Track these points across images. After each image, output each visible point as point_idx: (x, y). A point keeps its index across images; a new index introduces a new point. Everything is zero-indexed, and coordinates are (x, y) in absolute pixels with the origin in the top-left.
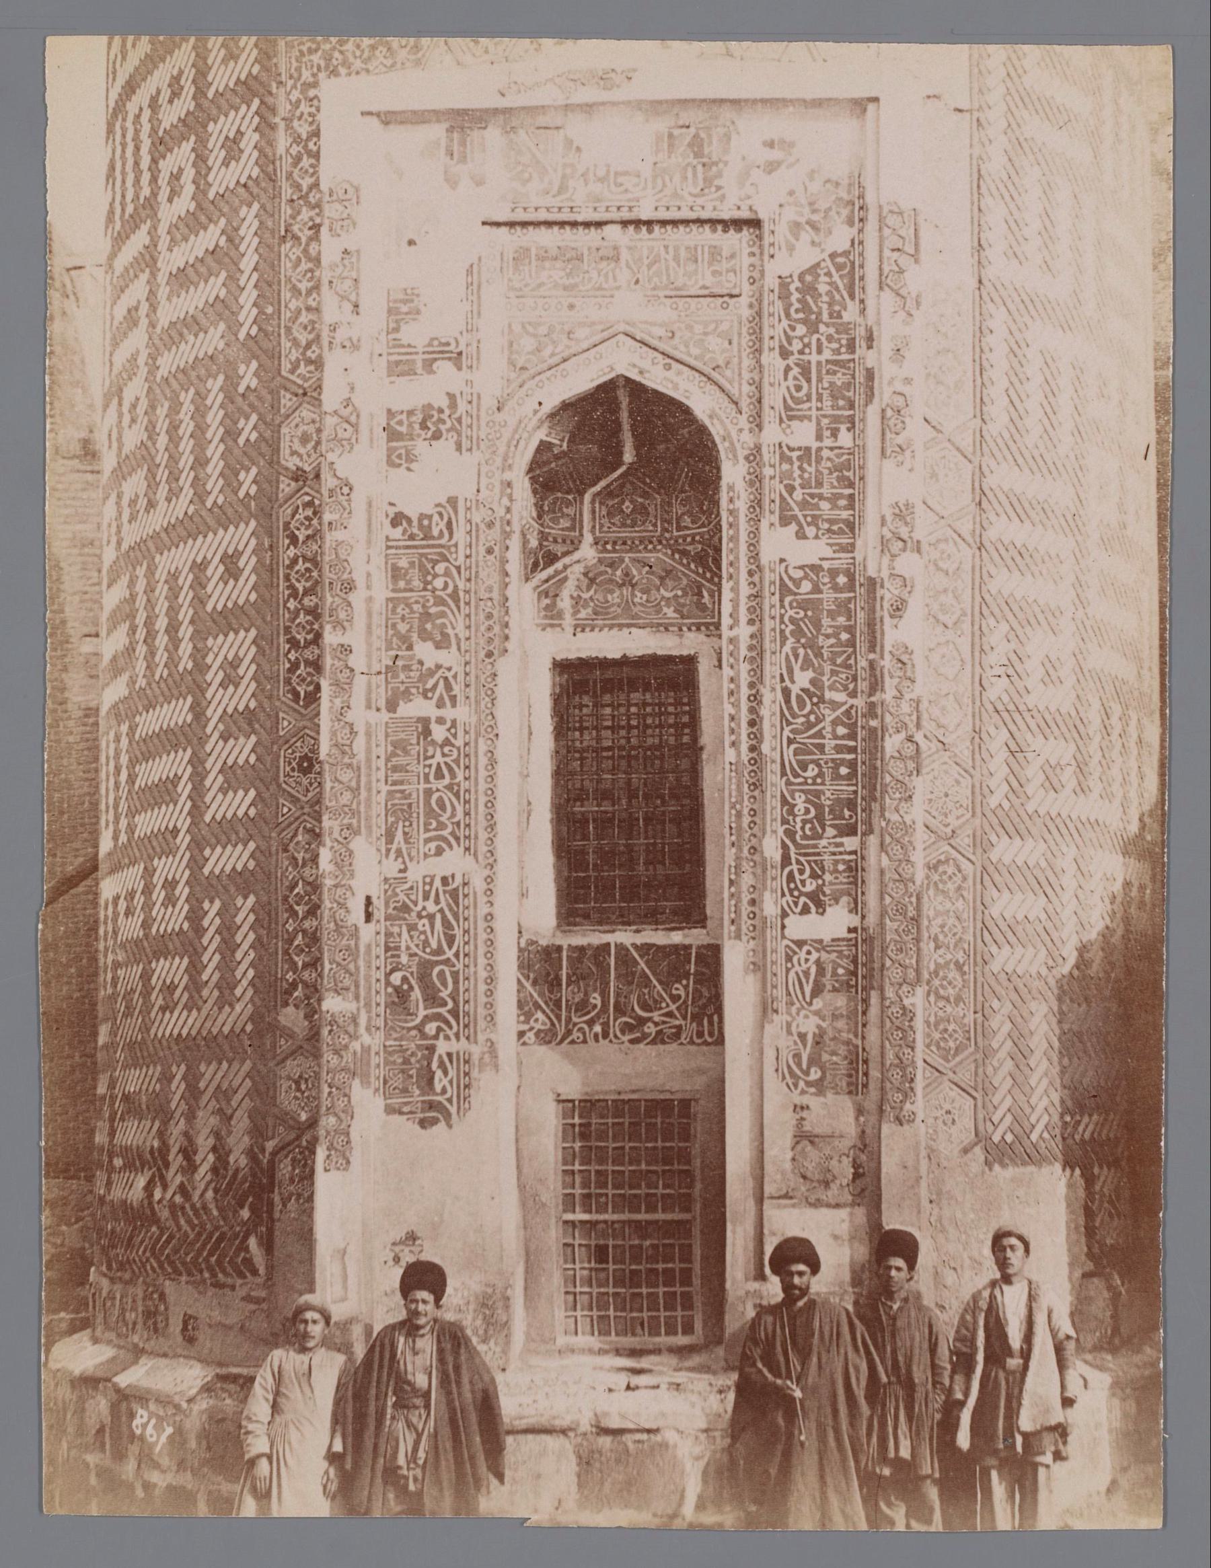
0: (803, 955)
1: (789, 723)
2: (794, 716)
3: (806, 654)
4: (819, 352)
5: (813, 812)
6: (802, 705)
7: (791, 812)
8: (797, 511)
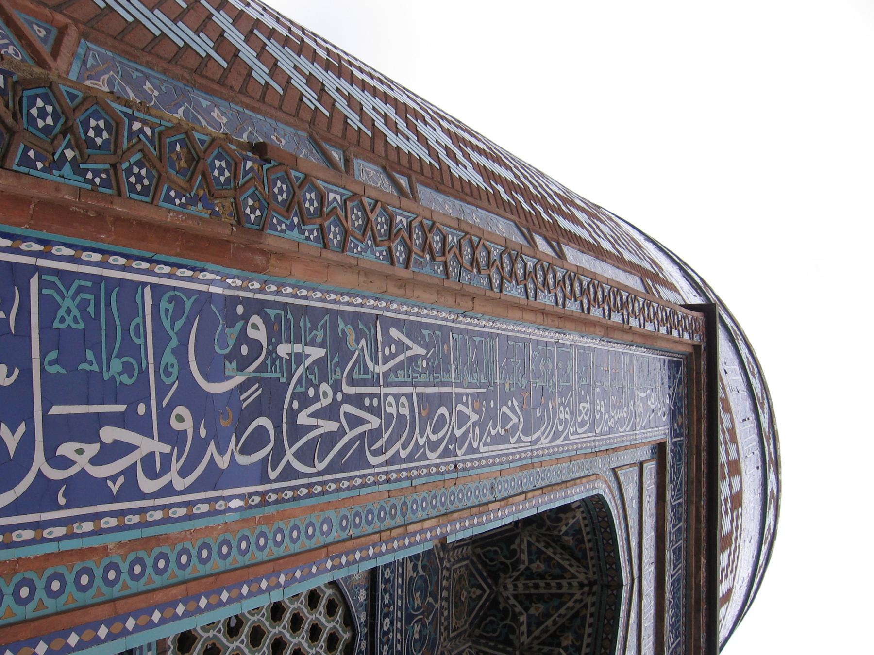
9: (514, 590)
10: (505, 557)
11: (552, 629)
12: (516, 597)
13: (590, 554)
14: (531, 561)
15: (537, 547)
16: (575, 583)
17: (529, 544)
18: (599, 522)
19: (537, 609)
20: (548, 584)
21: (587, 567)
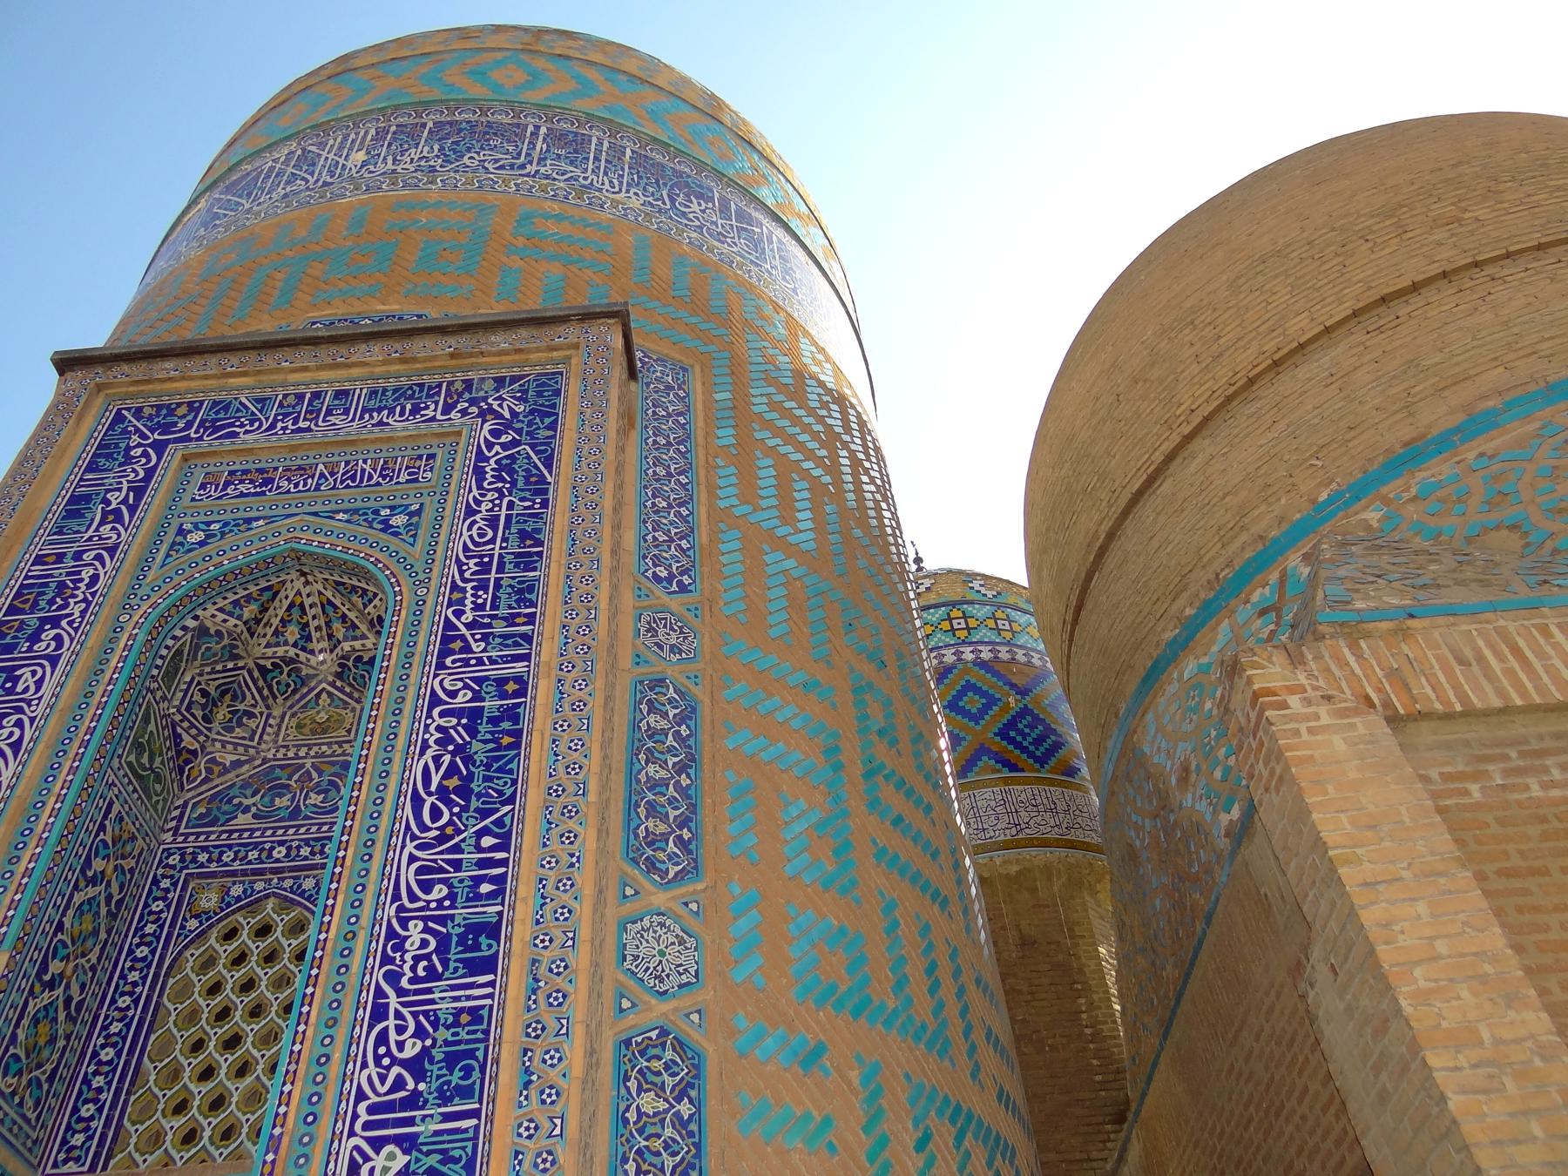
0: (379, 1161)
1: (414, 838)
2: (425, 829)
3: (453, 764)
4: (511, 505)
5: (433, 944)
6: (436, 814)
7: (399, 948)
8: (464, 630)
10: (281, 673)
11: (358, 614)
12: (332, 651)
13: (264, 584)
14: (286, 643)
16: (305, 591)
17: (268, 646)
19: (339, 630)
20: (314, 617)
21: (283, 582)
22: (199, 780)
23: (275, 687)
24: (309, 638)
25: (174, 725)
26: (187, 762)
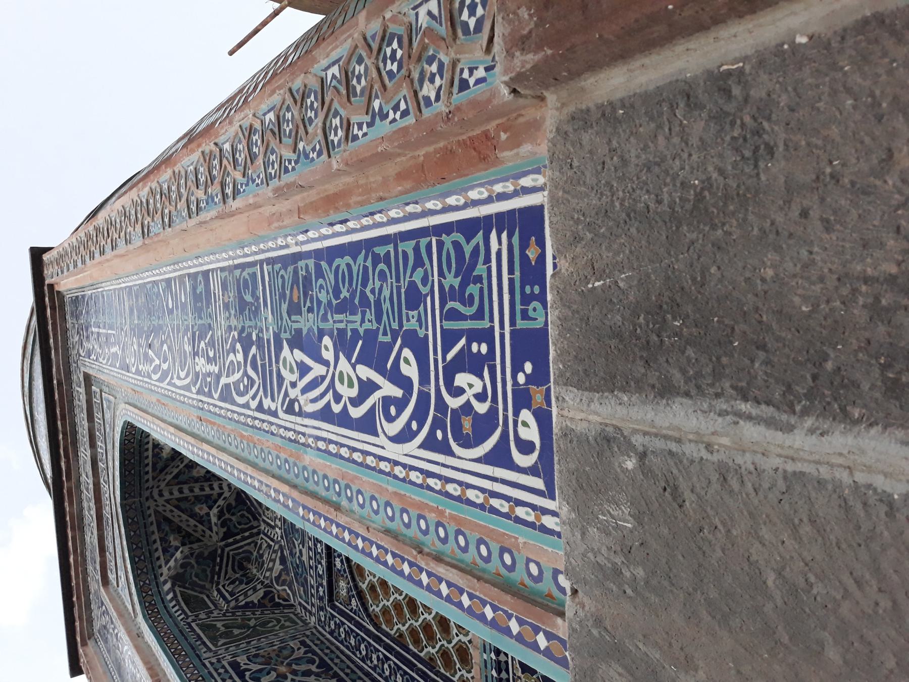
9: (222, 484)
10: (231, 520)
13: (154, 528)
15: (203, 526)
16: (166, 495)
17: (211, 529)
18: (146, 566)
20: (191, 491)
21: (156, 512)
22: (289, 591)
23: (243, 526)
24: (208, 497)
25: (237, 607)
26: (273, 599)
